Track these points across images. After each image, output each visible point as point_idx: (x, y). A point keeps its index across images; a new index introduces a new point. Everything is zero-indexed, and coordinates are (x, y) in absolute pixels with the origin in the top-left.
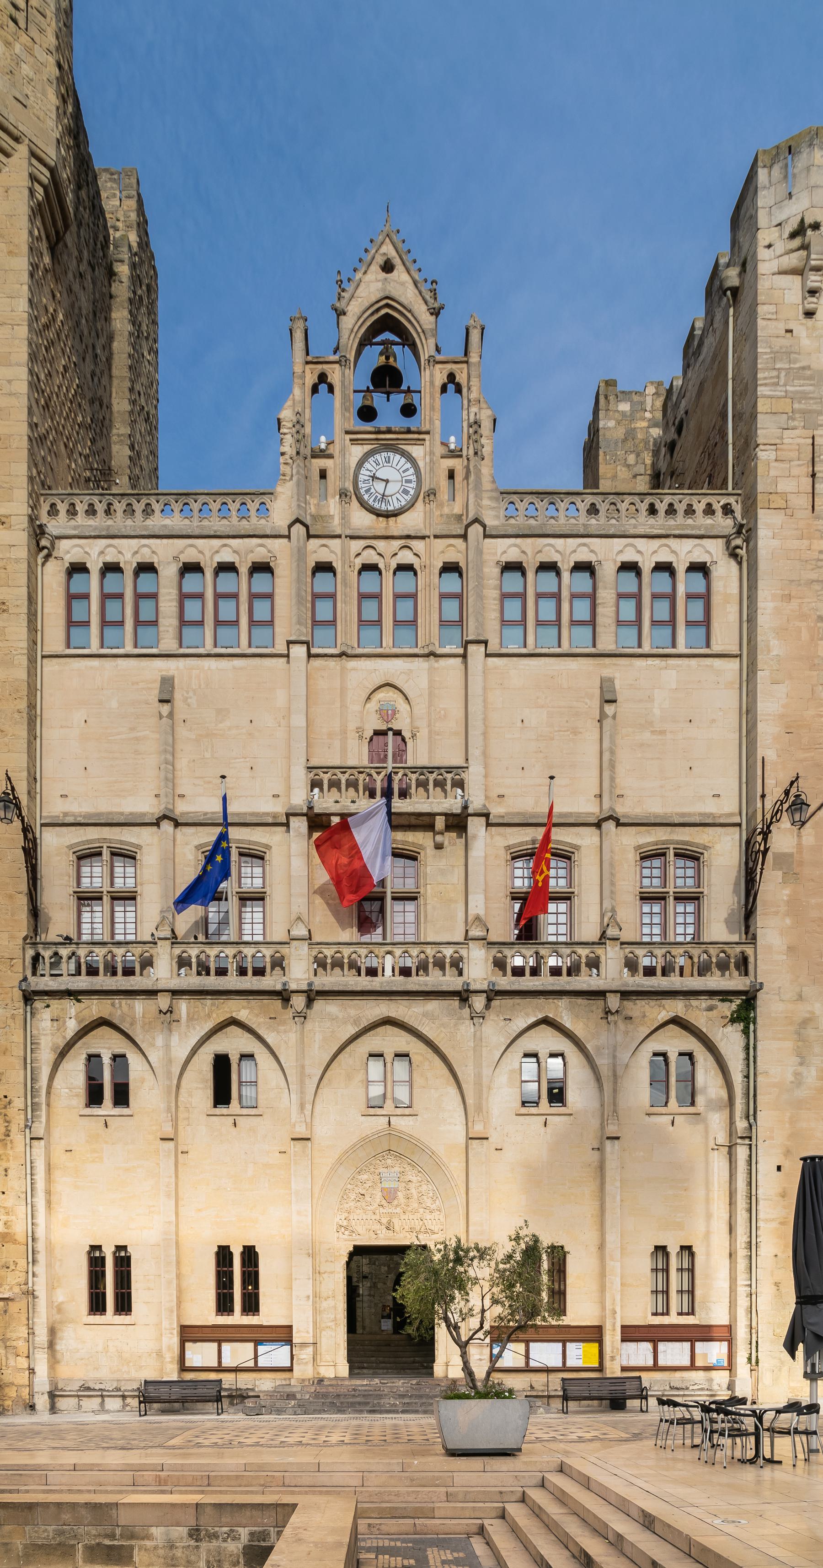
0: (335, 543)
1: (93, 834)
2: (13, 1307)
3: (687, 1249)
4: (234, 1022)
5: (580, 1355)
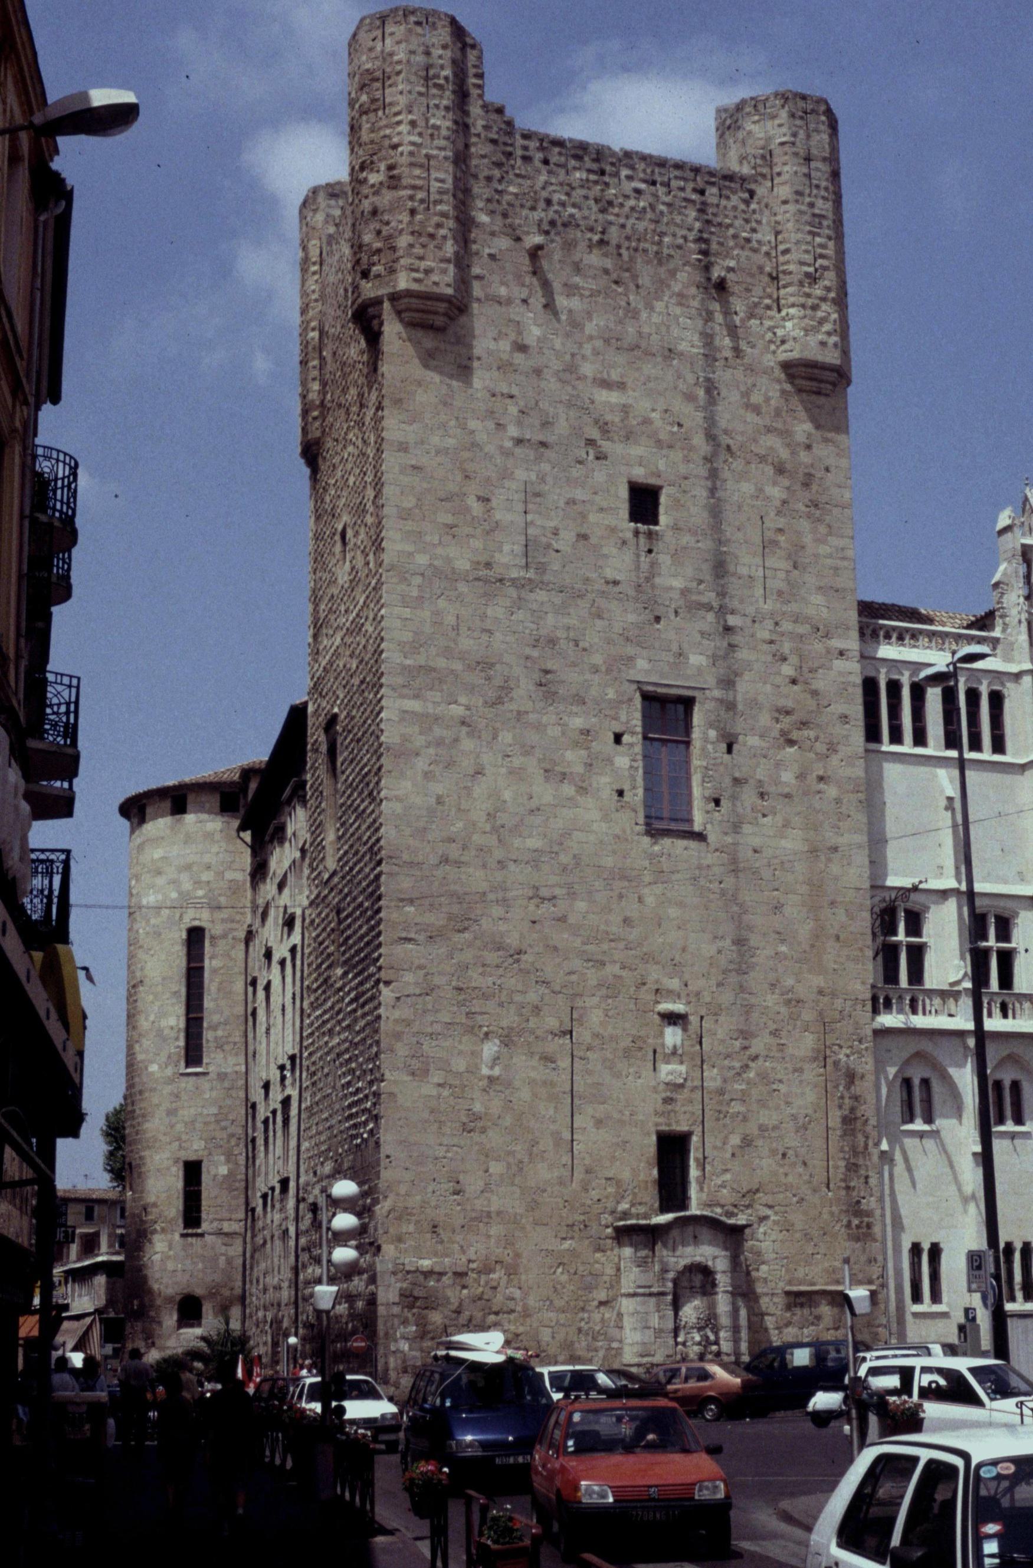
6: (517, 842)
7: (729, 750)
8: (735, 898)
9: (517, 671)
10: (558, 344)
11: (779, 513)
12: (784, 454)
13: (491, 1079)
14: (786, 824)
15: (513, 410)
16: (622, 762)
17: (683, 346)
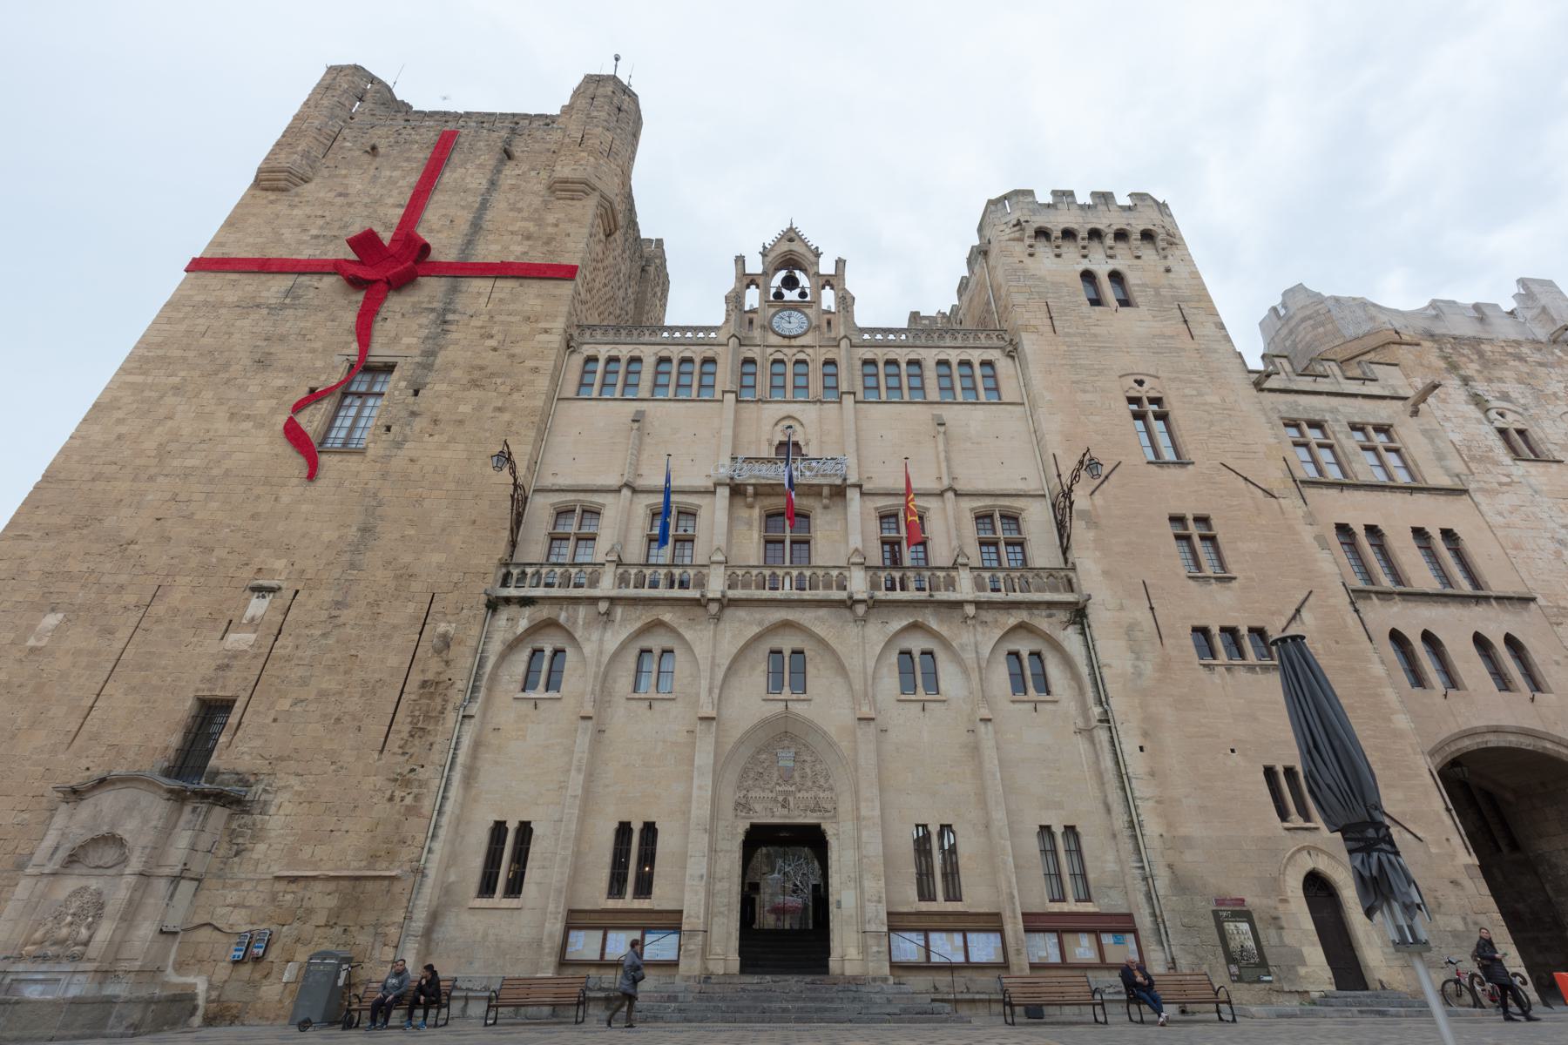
2: (397, 887)
3: (1070, 830)
4: (659, 624)
5: (984, 948)
6: (176, 463)
7: (416, 393)
8: (375, 495)
13: (33, 650)
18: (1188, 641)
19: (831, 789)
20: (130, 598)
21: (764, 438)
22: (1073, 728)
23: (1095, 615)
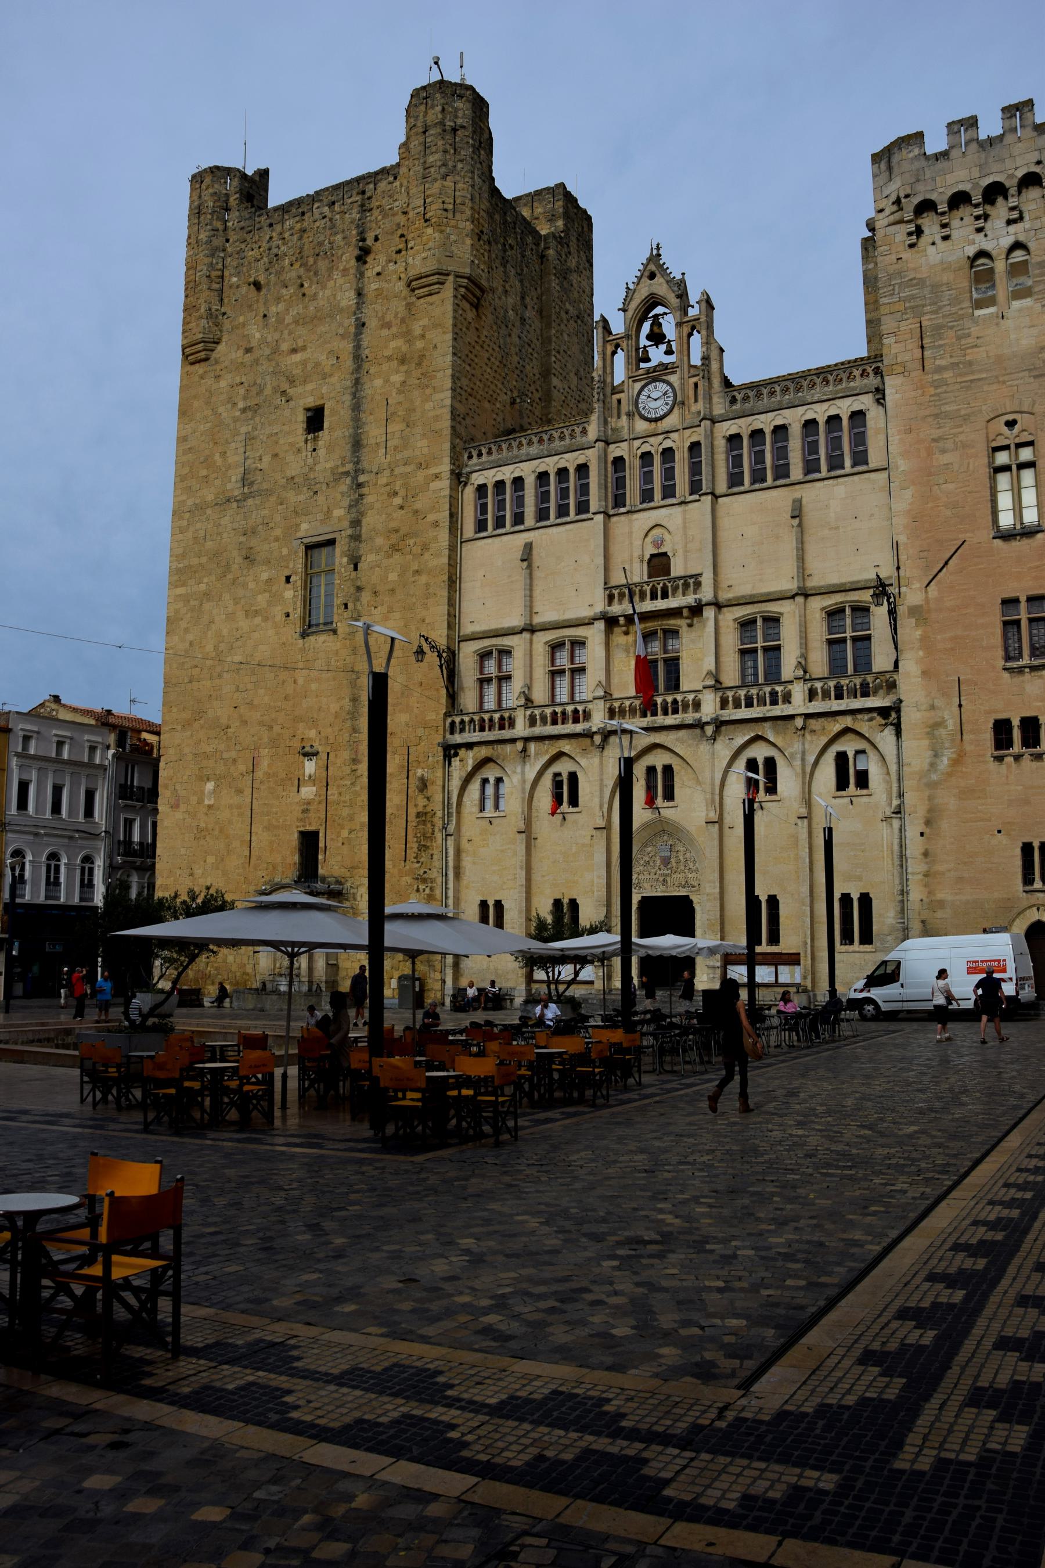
0: (624, 445)
1: (486, 643)
7: (356, 569)
9: (235, 553)
10: (269, 339)
11: (400, 392)
12: (404, 348)
13: (210, 807)
14: (391, 610)
15: (242, 391)
16: (289, 594)
17: (344, 303)
18: (988, 736)
19: (697, 870)
20: (242, 768)
21: (637, 553)
22: (881, 816)
23: (910, 716)
